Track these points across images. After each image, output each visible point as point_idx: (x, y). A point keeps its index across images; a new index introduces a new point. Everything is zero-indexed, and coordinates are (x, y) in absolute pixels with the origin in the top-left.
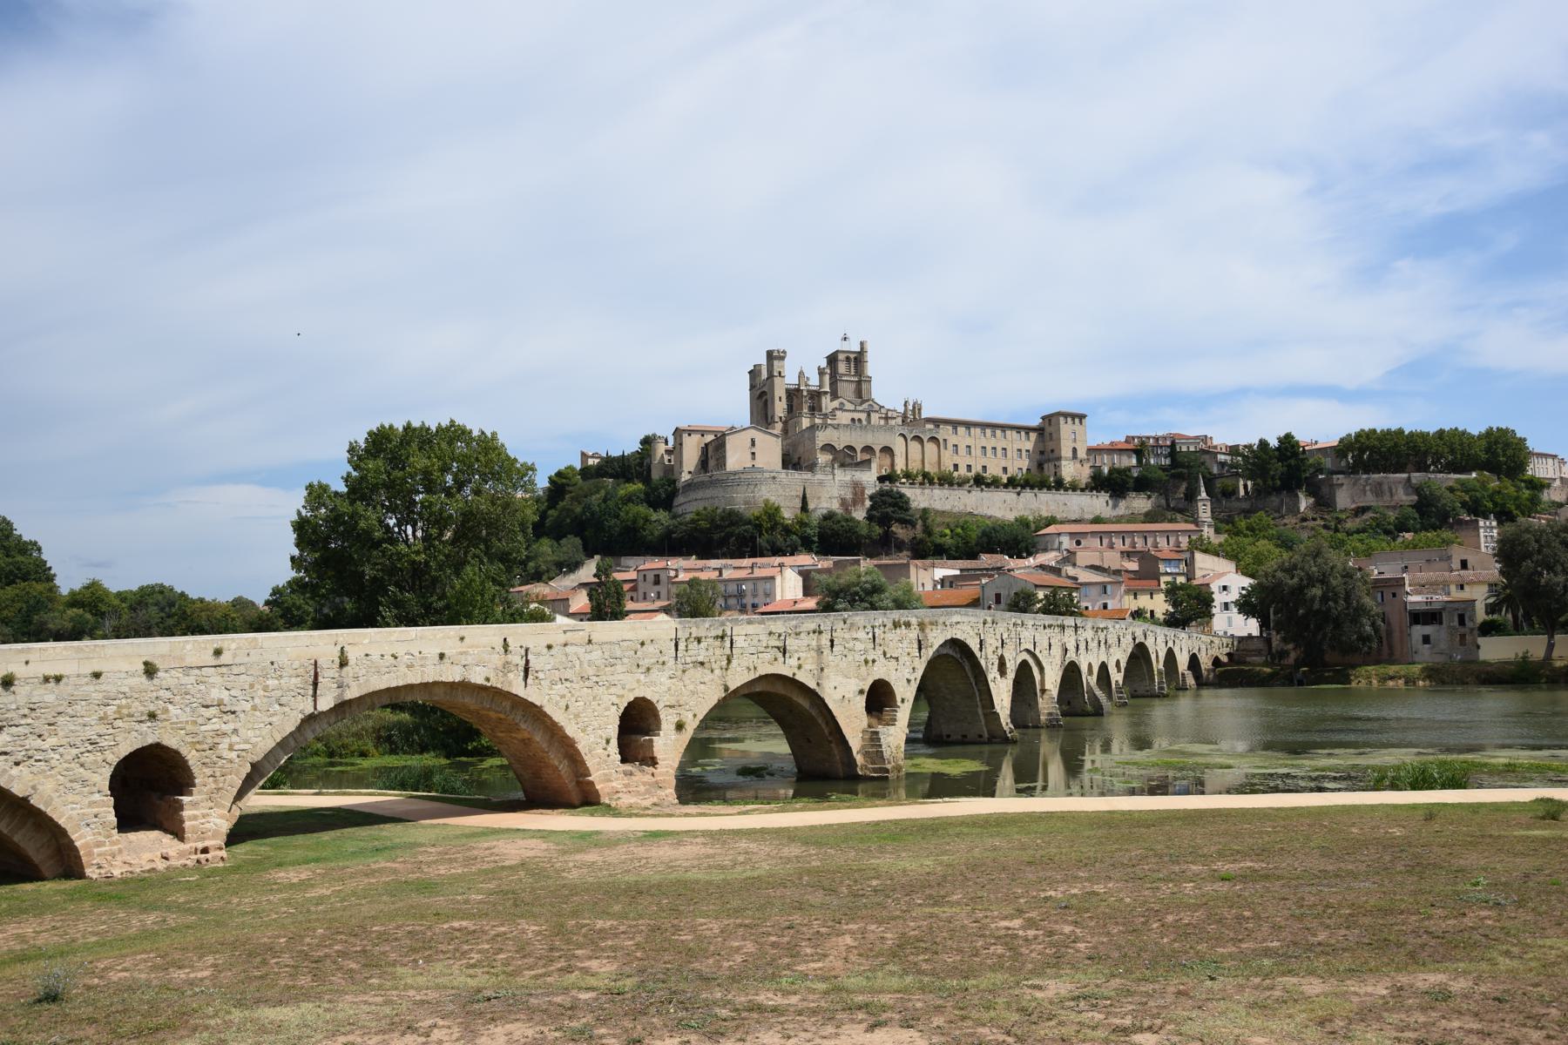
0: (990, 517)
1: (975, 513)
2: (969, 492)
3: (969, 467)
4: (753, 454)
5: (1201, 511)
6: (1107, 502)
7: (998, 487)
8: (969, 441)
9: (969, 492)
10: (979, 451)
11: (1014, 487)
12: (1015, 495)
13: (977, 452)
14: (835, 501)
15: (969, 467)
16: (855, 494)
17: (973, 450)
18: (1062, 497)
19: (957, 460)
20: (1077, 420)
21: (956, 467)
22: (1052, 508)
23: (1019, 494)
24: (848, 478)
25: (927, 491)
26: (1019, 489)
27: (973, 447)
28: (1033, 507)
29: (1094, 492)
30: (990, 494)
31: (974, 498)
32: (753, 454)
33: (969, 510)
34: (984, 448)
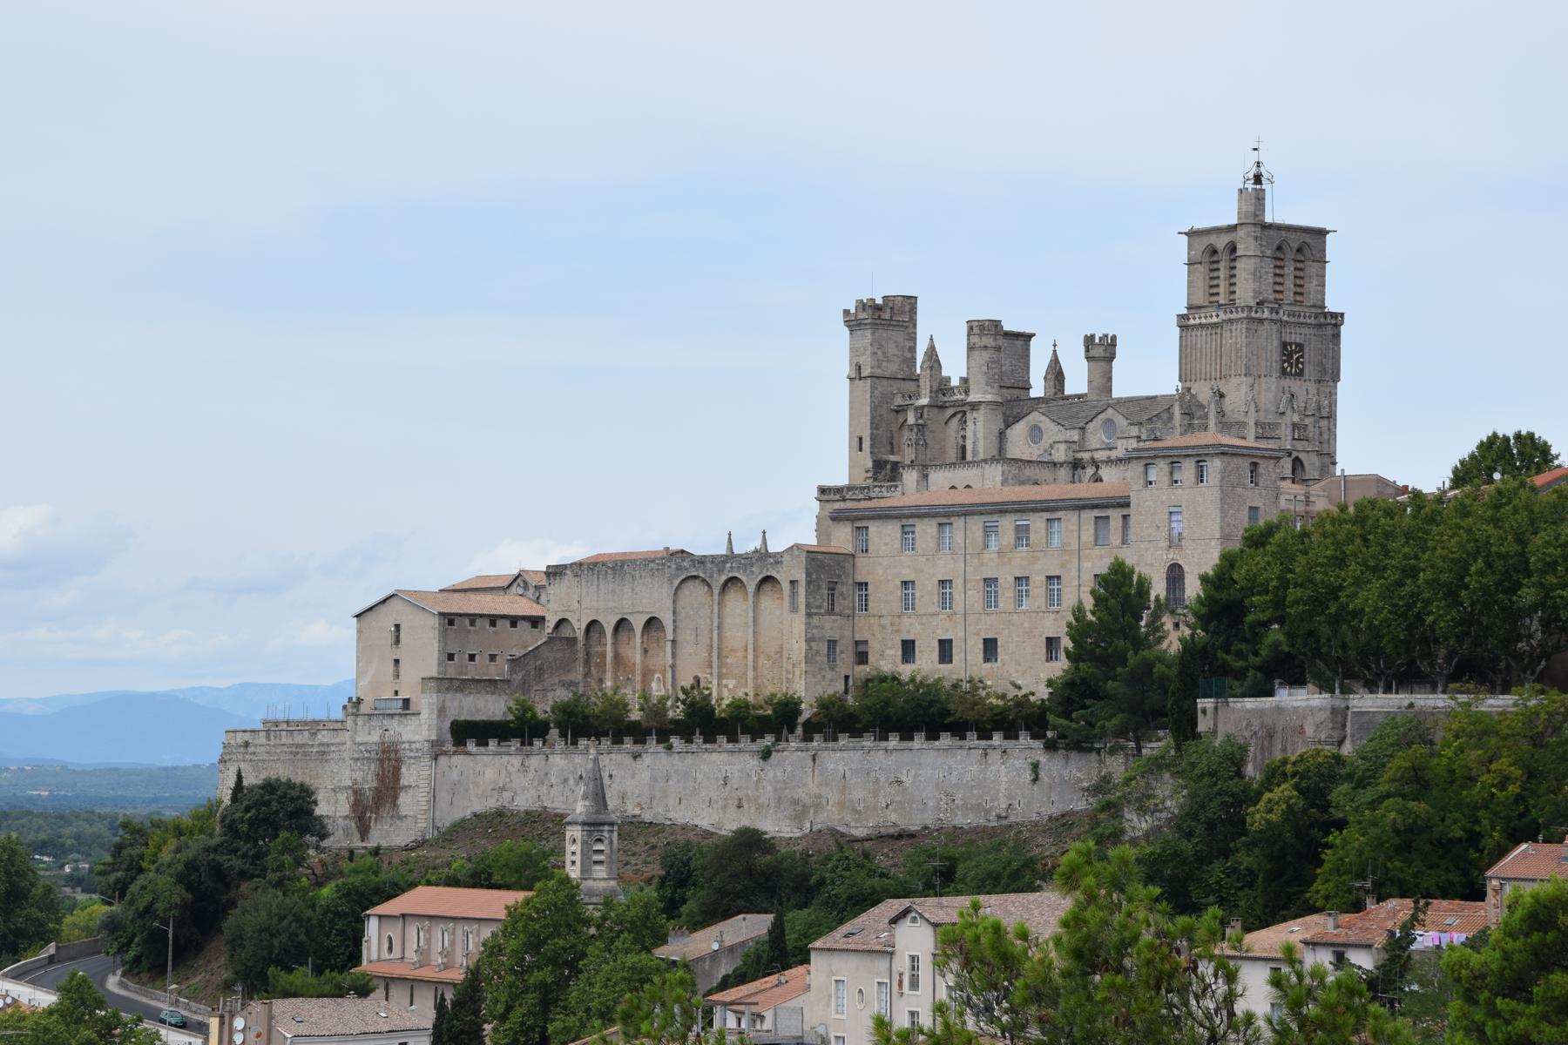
0: (684, 827)
1: (647, 817)
2: (636, 757)
3: (945, 650)
4: (397, 661)
5: (568, 864)
6: (1035, 767)
7: (710, 738)
8: (946, 567)
9: (636, 757)
10: (976, 596)
11: (756, 735)
12: (753, 762)
13: (968, 597)
14: (342, 797)
15: (945, 650)
16: (381, 777)
17: (958, 596)
18: (890, 761)
19: (911, 628)
20: (1188, 470)
21: (908, 649)
22: (858, 794)
23: (766, 755)
24: (375, 737)
25: (534, 762)
26: (768, 740)
27: (958, 583)
28: (801, 794)
29: (997, 739)
30: (689, 759)
31: (645, 776)
32: (397, 661)
33: (633, 810)
34: (990, 582)
